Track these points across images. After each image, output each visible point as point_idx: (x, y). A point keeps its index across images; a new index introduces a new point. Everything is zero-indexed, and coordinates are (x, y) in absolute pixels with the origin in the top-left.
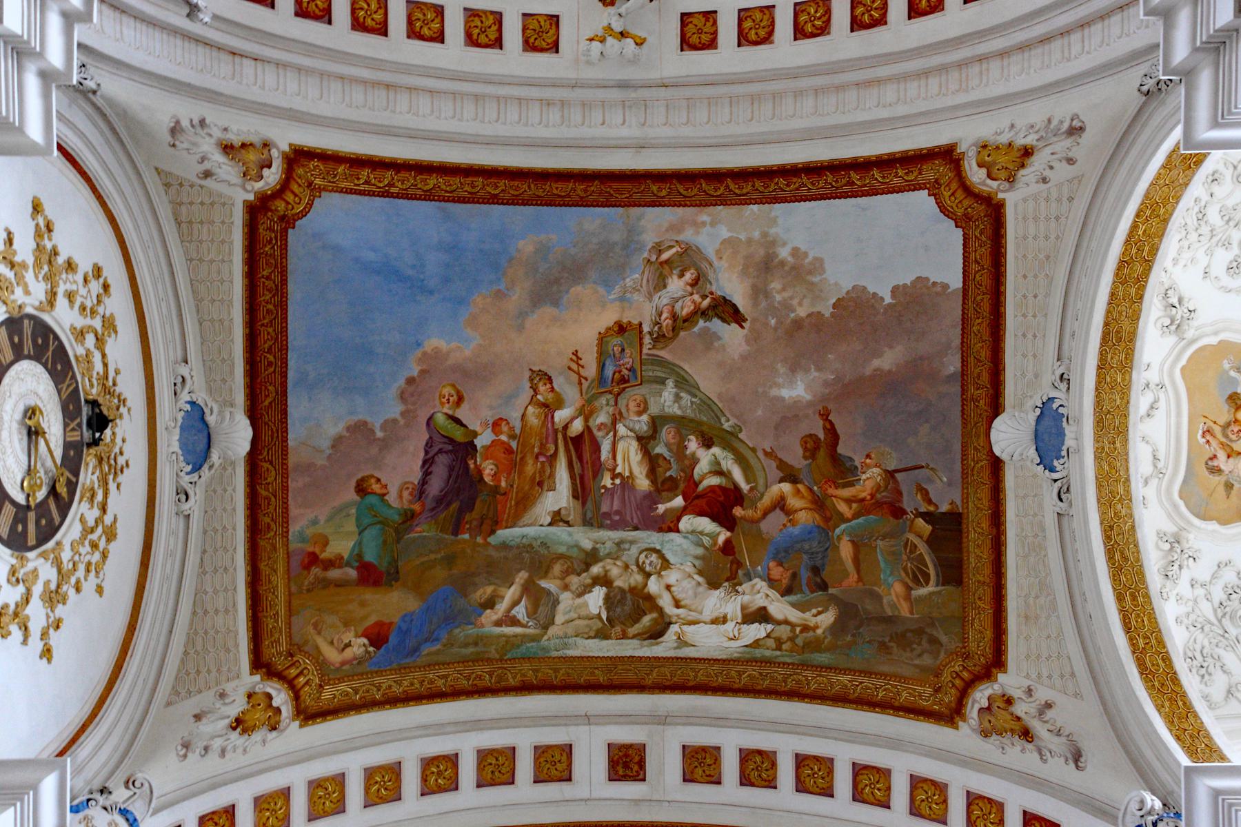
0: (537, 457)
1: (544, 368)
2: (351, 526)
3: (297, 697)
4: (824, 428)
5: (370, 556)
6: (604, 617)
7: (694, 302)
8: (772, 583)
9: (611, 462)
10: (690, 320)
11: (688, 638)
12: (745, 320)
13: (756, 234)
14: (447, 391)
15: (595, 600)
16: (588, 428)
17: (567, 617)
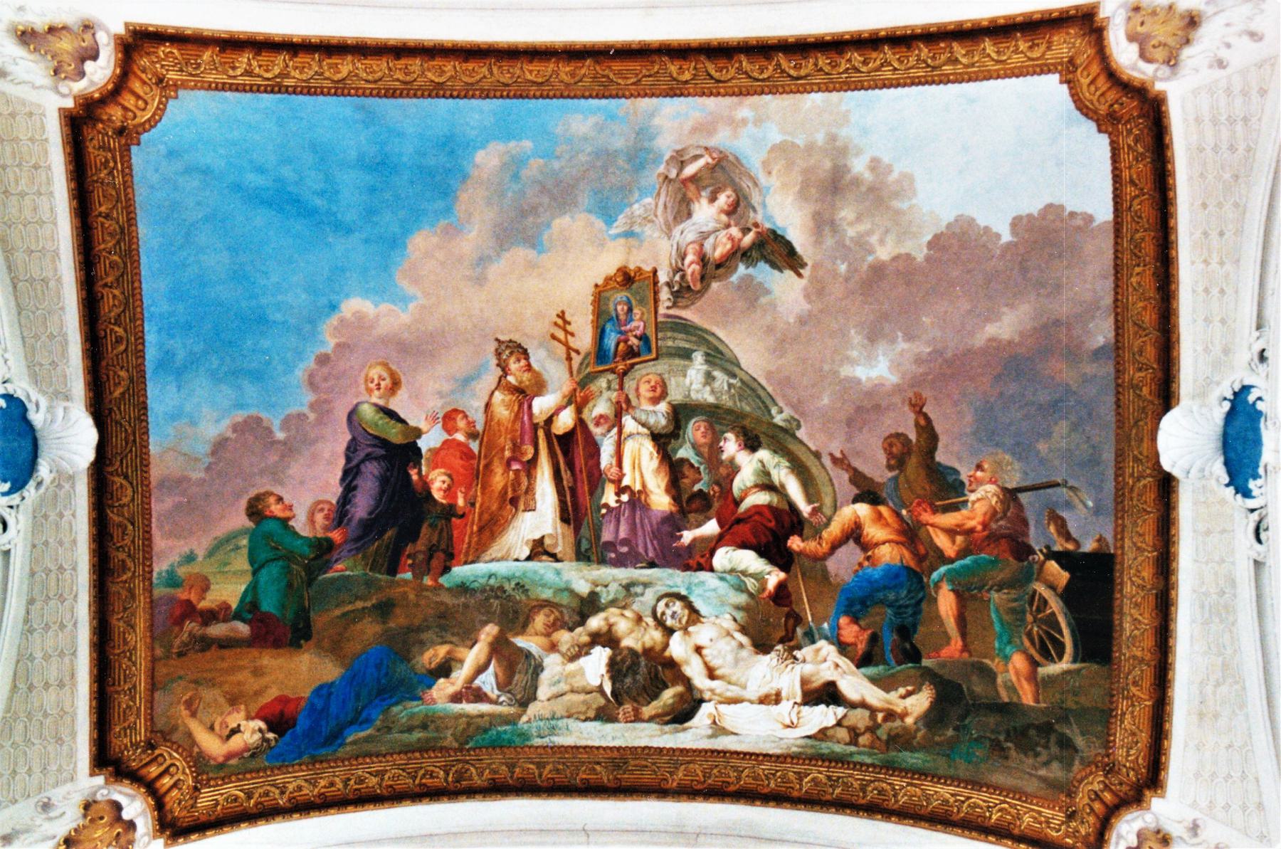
0: (508, 464)
1: (516, 337)
2: (241, 563)
3: (159, 805)
4: (917, 424)
5: (269, 604)
6: (608, 689)
7: (731, 238)
8: (843, 648)
9: (614, 470)
10: (724, 265)
11: (727, 724)
12: (803, 265)
13: (820, 138)
14: (375, 372)
15: (595, 665)
16: (580, 423)
17: (555, 690)
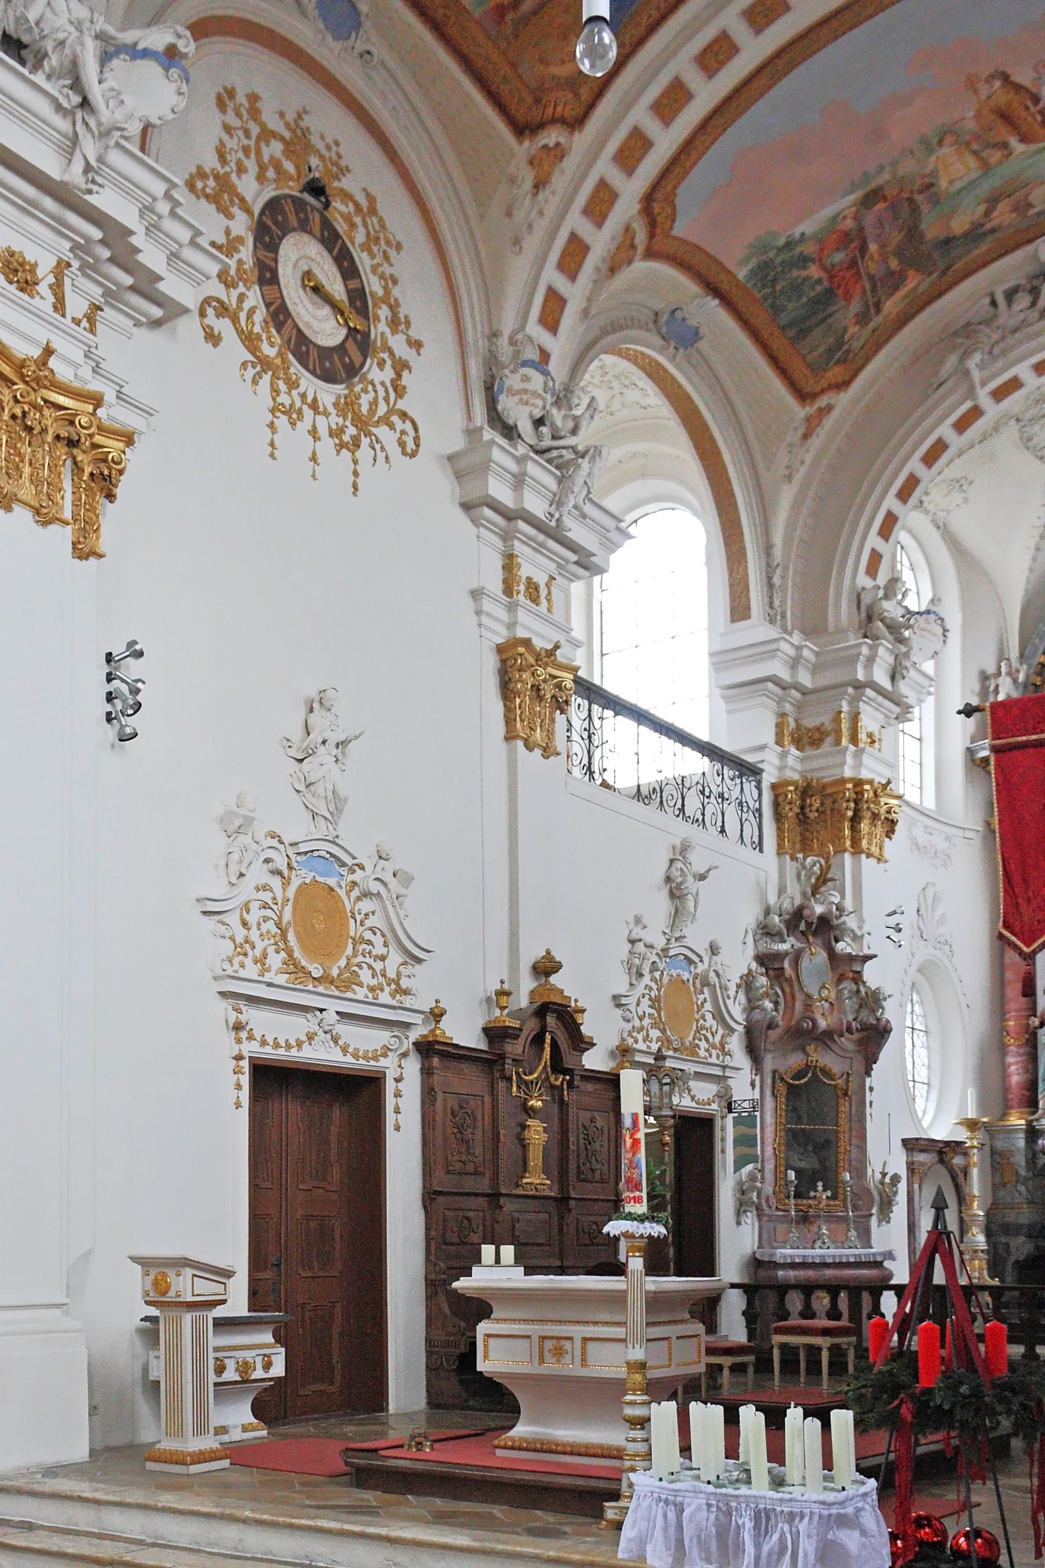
3: (563, 121)
